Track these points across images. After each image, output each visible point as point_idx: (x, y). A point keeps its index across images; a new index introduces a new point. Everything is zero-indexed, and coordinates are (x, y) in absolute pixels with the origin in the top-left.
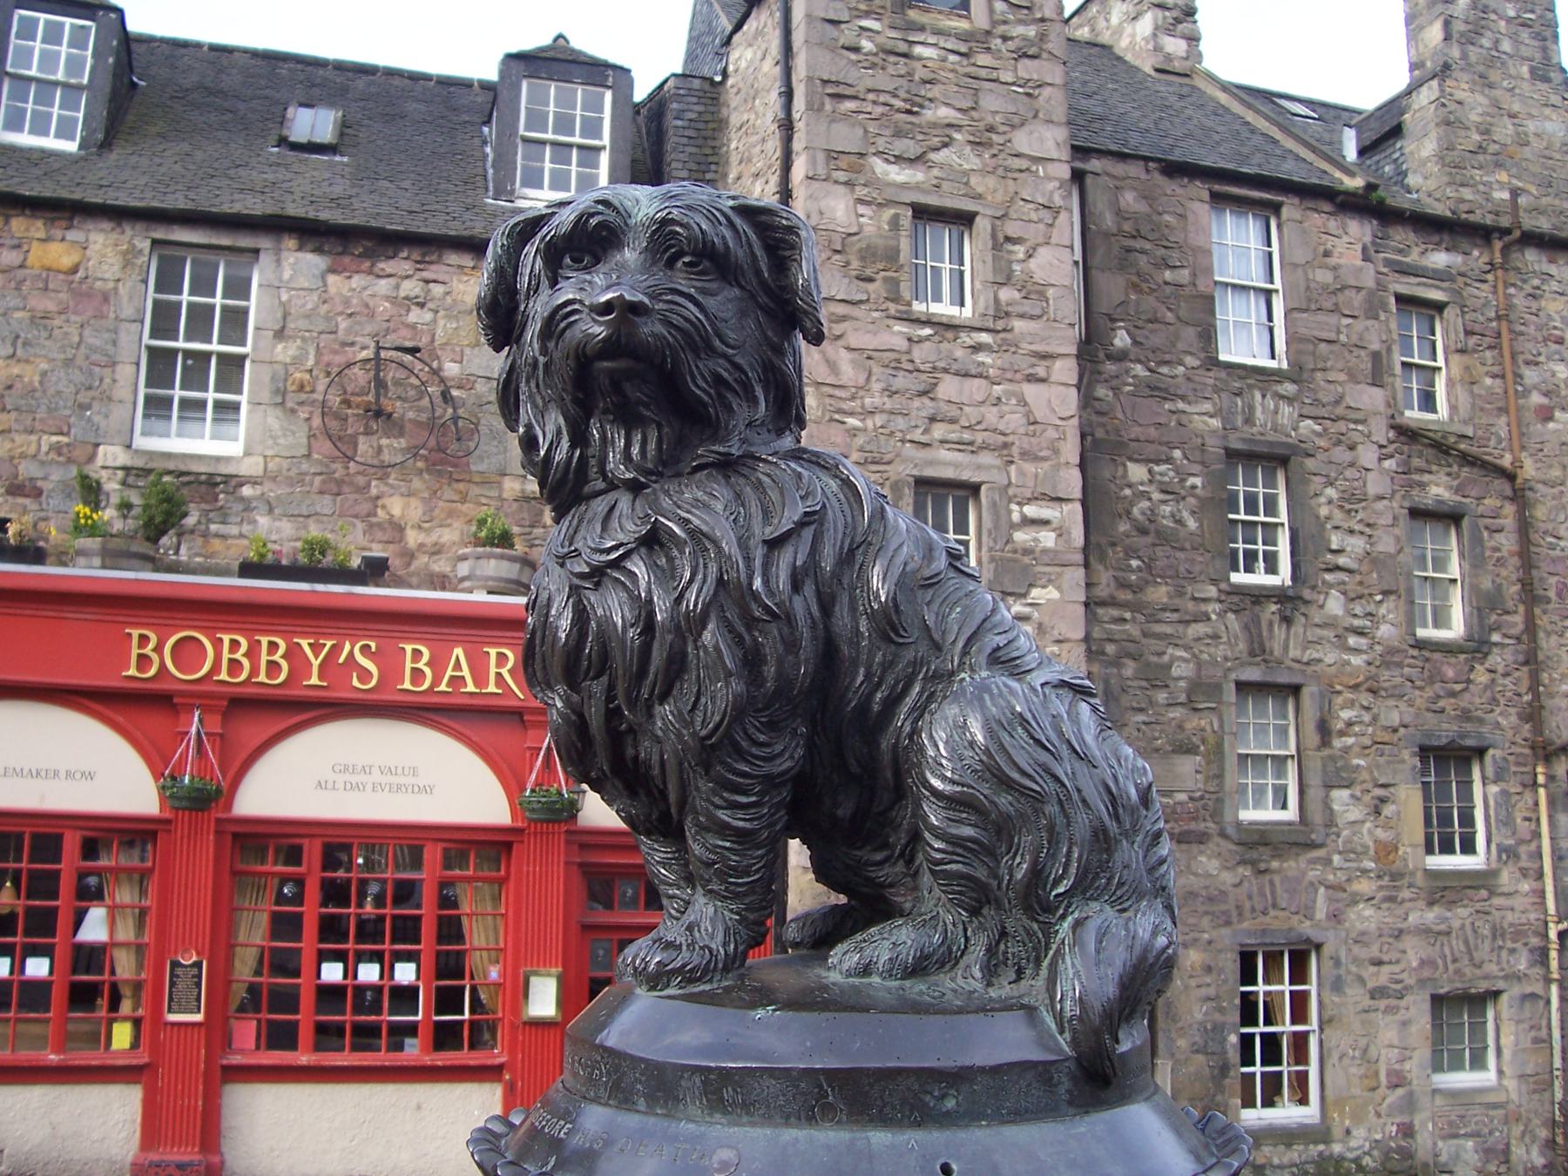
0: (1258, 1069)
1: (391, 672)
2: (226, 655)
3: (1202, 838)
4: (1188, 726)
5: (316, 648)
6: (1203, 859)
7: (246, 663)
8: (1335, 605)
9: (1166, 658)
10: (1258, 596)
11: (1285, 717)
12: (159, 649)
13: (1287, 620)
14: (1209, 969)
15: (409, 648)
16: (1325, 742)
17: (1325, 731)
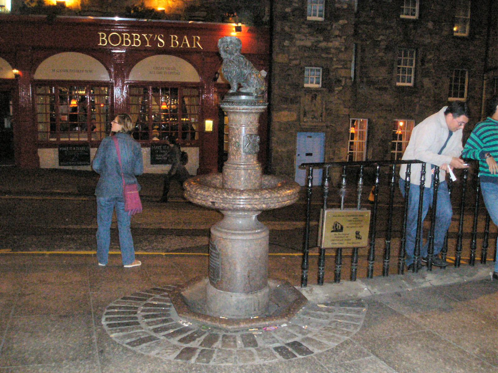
0: (396, 152)
1: (168, 41)
2: (124, 39)
3: (385, 89)
4: (385, 59)
5: (148, 36)
6: (385, 95)
7: (130, 41)
8: (430, 25)
9: (379, 39)
10: (409, 21)
11: (413, 57)
12: (107, 38)
13: (415, 28)
14: (384, 125)
15: (172, 36)
16: (423, 64)
17: (423, 61)
